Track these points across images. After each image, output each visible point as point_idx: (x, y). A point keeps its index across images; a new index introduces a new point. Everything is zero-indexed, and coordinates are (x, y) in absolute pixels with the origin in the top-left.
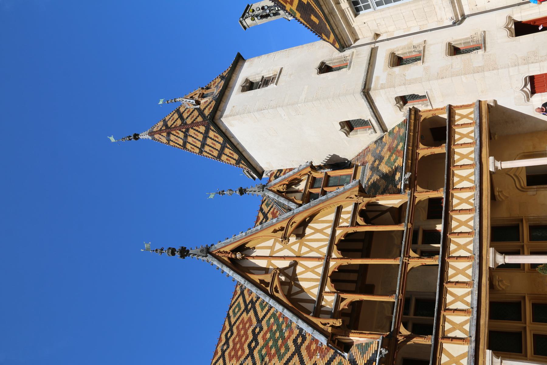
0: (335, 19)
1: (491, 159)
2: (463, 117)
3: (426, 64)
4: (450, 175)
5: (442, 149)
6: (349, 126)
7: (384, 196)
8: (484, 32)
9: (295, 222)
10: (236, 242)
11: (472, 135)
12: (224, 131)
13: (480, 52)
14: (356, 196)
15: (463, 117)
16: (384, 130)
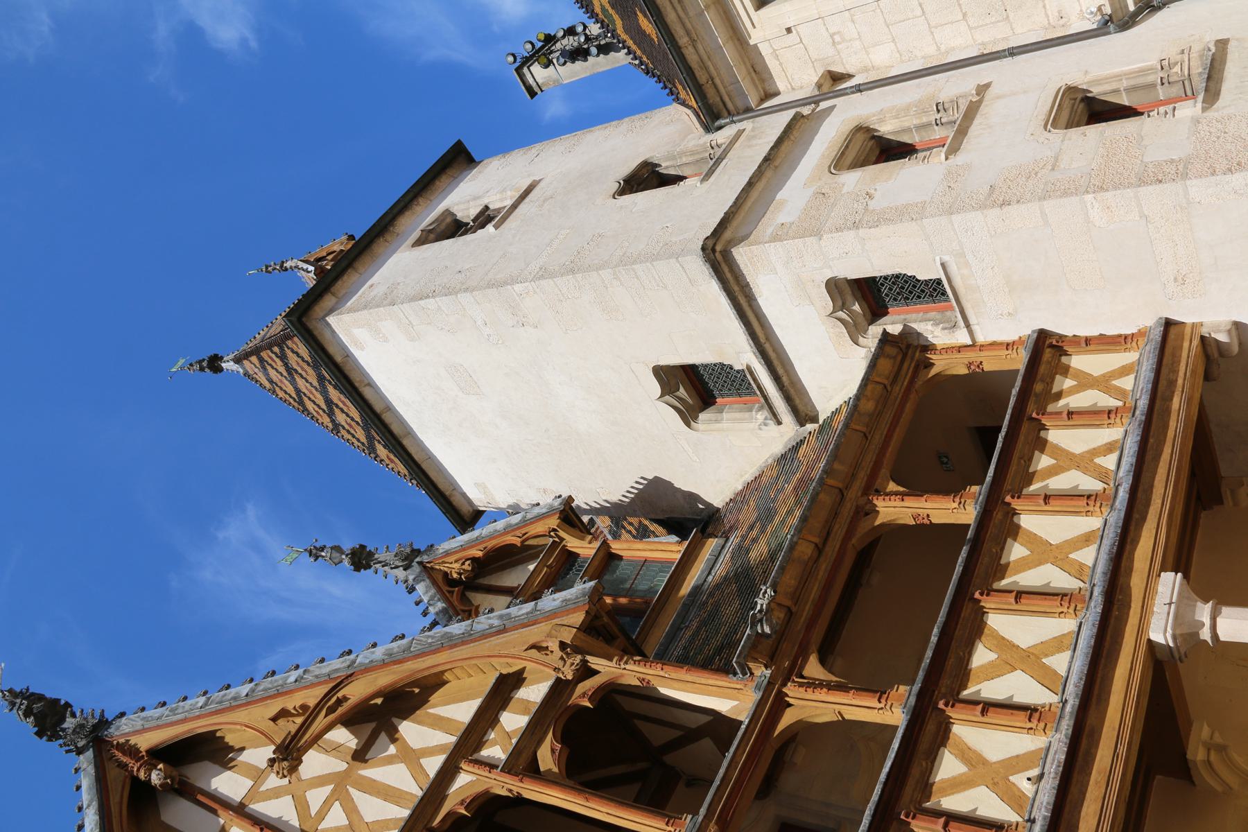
0: (684, 9)
1: (1169, 583)
2: (1086, 382)
3: (959, 159)
4: (965, 627)
5: (958, 511)
6: (695, 389)
7: (682, 674)
8: (1222, 44)
9: (345, 699)
10: (158, 727)
11: (1109, 462)
12: (338, 359)
13: (1188, 110)
14: (563, 646)
15: (1086, 382)
16: (803, 413)
